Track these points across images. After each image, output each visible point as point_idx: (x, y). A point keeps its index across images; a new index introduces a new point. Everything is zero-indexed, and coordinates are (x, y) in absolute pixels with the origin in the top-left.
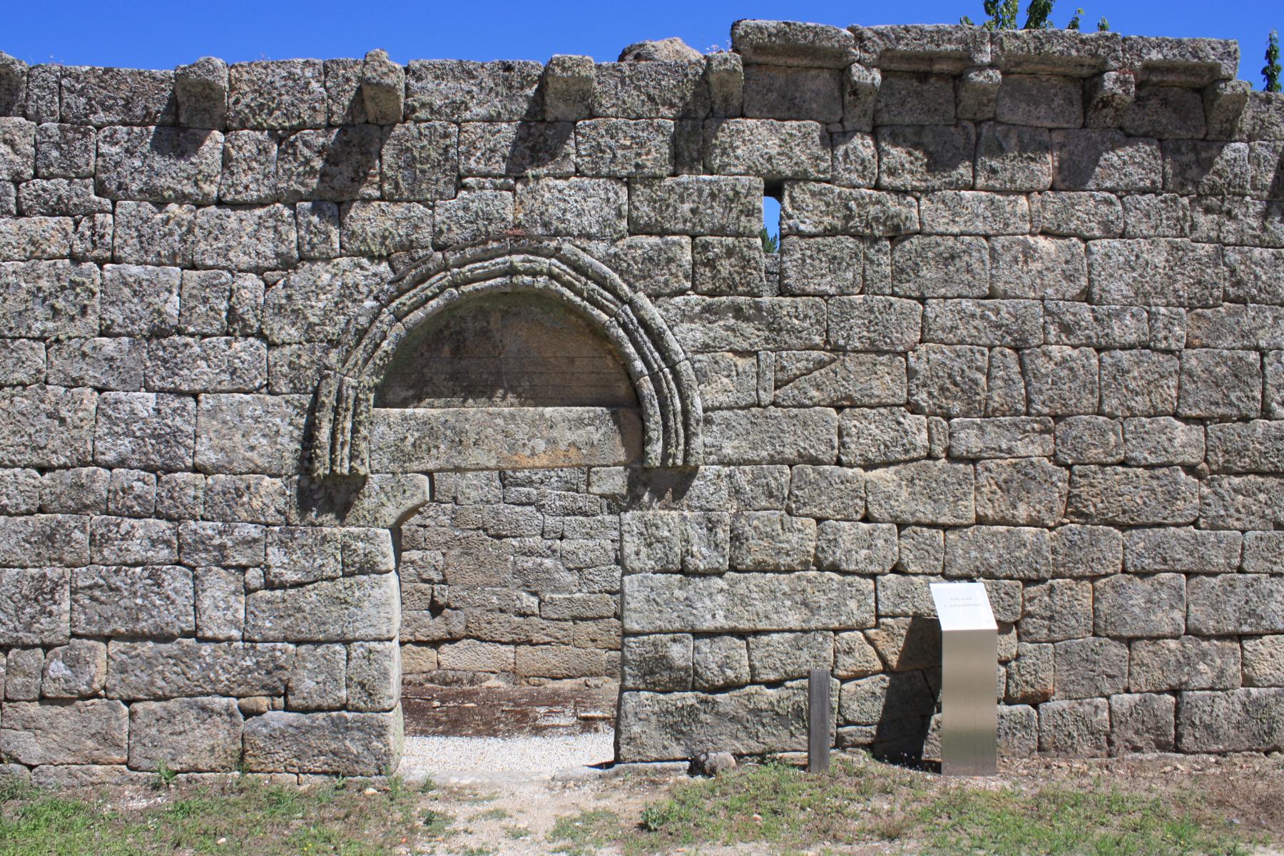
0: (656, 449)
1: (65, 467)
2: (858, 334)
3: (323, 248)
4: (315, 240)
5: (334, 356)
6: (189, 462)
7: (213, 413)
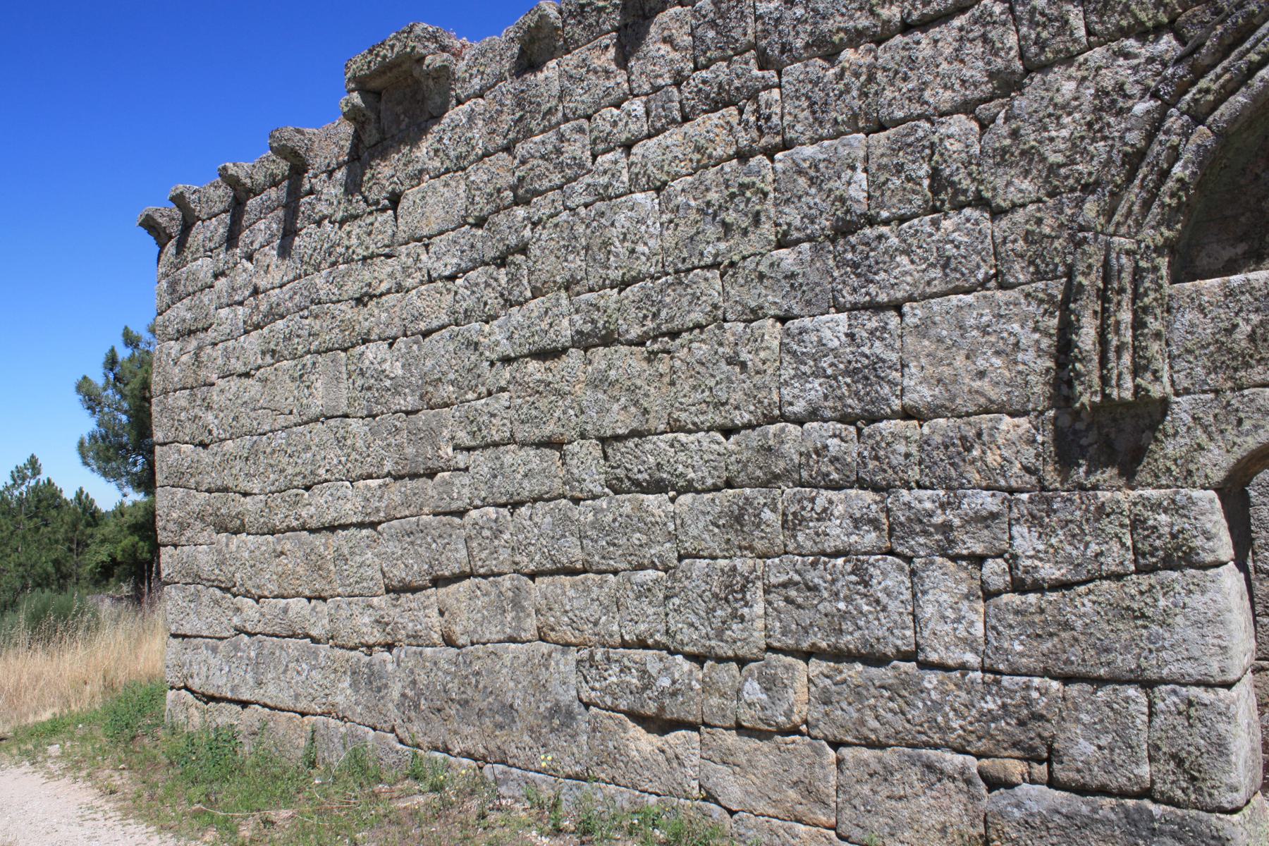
1: (750, 426)
3: (1058, 43)
4: (1045, 35)
5: (1091, 208)
6: (896, 404)
7: (922, 330)
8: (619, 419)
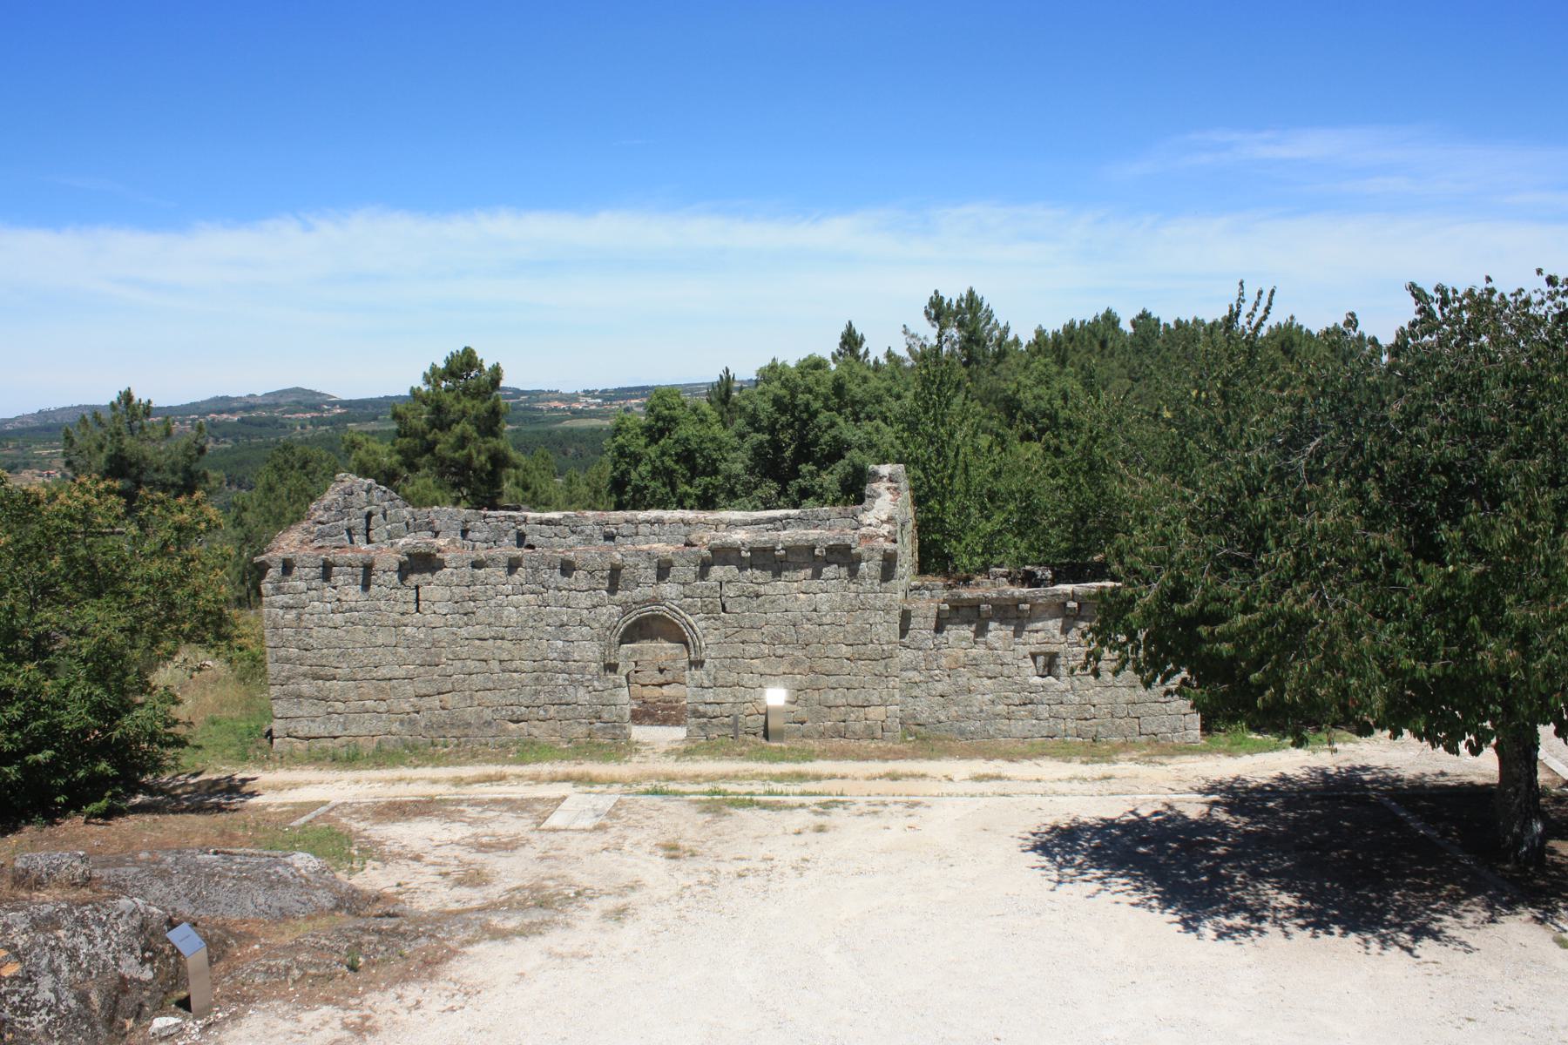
0: (693, 656)
2: (747, 623)
8: (505, 656)
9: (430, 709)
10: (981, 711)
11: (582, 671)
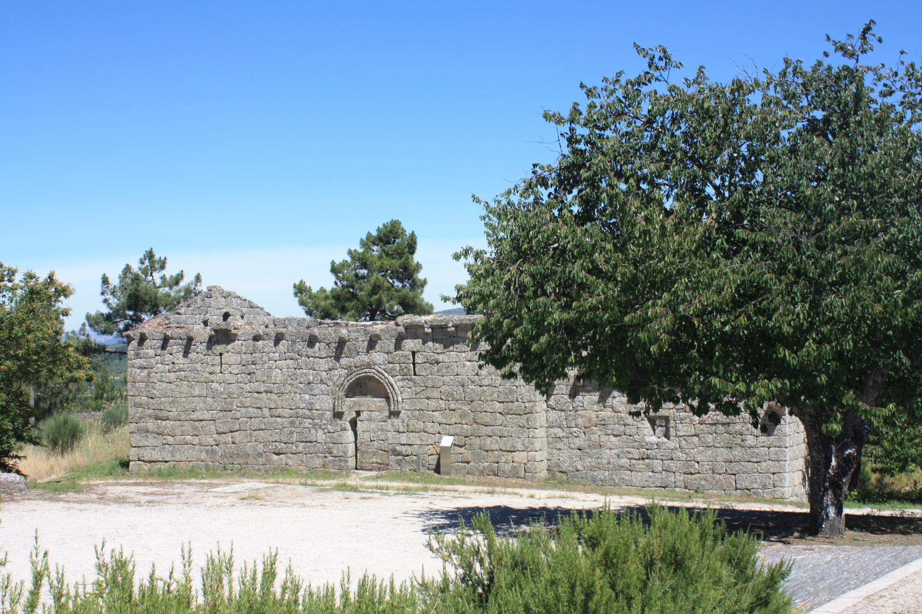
0: (392, 407)
2: (430, 384)
7: (319, 399)
9: (225, 443)
10: (609, 463)
11: (321, 417)
